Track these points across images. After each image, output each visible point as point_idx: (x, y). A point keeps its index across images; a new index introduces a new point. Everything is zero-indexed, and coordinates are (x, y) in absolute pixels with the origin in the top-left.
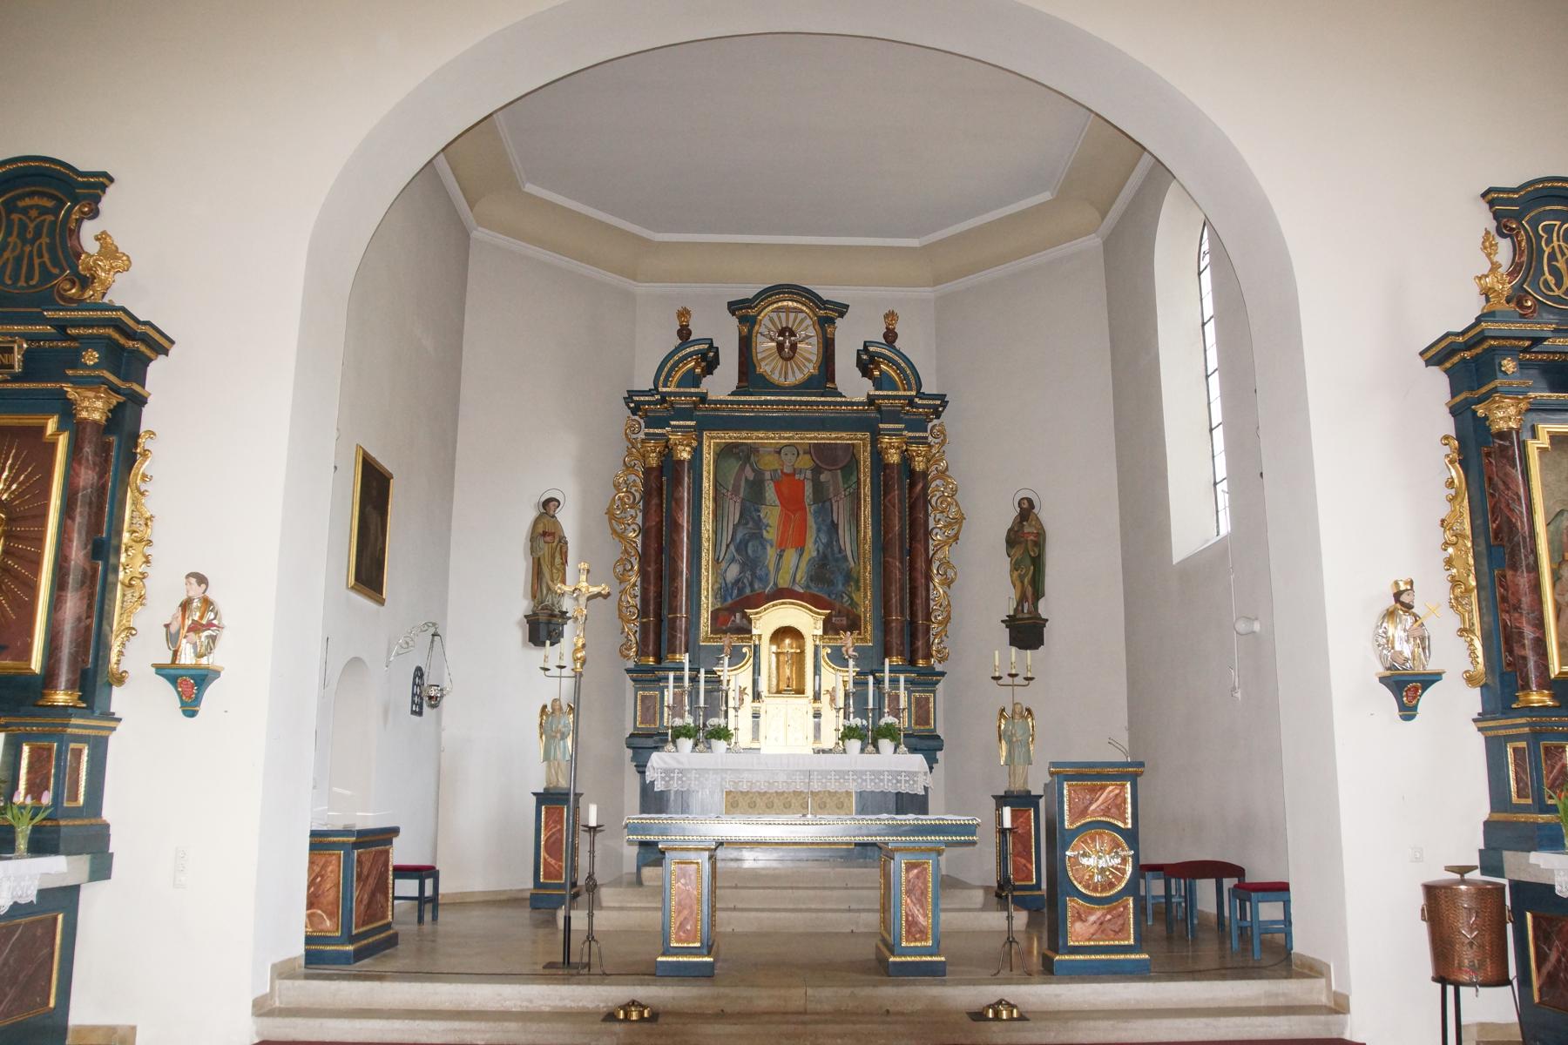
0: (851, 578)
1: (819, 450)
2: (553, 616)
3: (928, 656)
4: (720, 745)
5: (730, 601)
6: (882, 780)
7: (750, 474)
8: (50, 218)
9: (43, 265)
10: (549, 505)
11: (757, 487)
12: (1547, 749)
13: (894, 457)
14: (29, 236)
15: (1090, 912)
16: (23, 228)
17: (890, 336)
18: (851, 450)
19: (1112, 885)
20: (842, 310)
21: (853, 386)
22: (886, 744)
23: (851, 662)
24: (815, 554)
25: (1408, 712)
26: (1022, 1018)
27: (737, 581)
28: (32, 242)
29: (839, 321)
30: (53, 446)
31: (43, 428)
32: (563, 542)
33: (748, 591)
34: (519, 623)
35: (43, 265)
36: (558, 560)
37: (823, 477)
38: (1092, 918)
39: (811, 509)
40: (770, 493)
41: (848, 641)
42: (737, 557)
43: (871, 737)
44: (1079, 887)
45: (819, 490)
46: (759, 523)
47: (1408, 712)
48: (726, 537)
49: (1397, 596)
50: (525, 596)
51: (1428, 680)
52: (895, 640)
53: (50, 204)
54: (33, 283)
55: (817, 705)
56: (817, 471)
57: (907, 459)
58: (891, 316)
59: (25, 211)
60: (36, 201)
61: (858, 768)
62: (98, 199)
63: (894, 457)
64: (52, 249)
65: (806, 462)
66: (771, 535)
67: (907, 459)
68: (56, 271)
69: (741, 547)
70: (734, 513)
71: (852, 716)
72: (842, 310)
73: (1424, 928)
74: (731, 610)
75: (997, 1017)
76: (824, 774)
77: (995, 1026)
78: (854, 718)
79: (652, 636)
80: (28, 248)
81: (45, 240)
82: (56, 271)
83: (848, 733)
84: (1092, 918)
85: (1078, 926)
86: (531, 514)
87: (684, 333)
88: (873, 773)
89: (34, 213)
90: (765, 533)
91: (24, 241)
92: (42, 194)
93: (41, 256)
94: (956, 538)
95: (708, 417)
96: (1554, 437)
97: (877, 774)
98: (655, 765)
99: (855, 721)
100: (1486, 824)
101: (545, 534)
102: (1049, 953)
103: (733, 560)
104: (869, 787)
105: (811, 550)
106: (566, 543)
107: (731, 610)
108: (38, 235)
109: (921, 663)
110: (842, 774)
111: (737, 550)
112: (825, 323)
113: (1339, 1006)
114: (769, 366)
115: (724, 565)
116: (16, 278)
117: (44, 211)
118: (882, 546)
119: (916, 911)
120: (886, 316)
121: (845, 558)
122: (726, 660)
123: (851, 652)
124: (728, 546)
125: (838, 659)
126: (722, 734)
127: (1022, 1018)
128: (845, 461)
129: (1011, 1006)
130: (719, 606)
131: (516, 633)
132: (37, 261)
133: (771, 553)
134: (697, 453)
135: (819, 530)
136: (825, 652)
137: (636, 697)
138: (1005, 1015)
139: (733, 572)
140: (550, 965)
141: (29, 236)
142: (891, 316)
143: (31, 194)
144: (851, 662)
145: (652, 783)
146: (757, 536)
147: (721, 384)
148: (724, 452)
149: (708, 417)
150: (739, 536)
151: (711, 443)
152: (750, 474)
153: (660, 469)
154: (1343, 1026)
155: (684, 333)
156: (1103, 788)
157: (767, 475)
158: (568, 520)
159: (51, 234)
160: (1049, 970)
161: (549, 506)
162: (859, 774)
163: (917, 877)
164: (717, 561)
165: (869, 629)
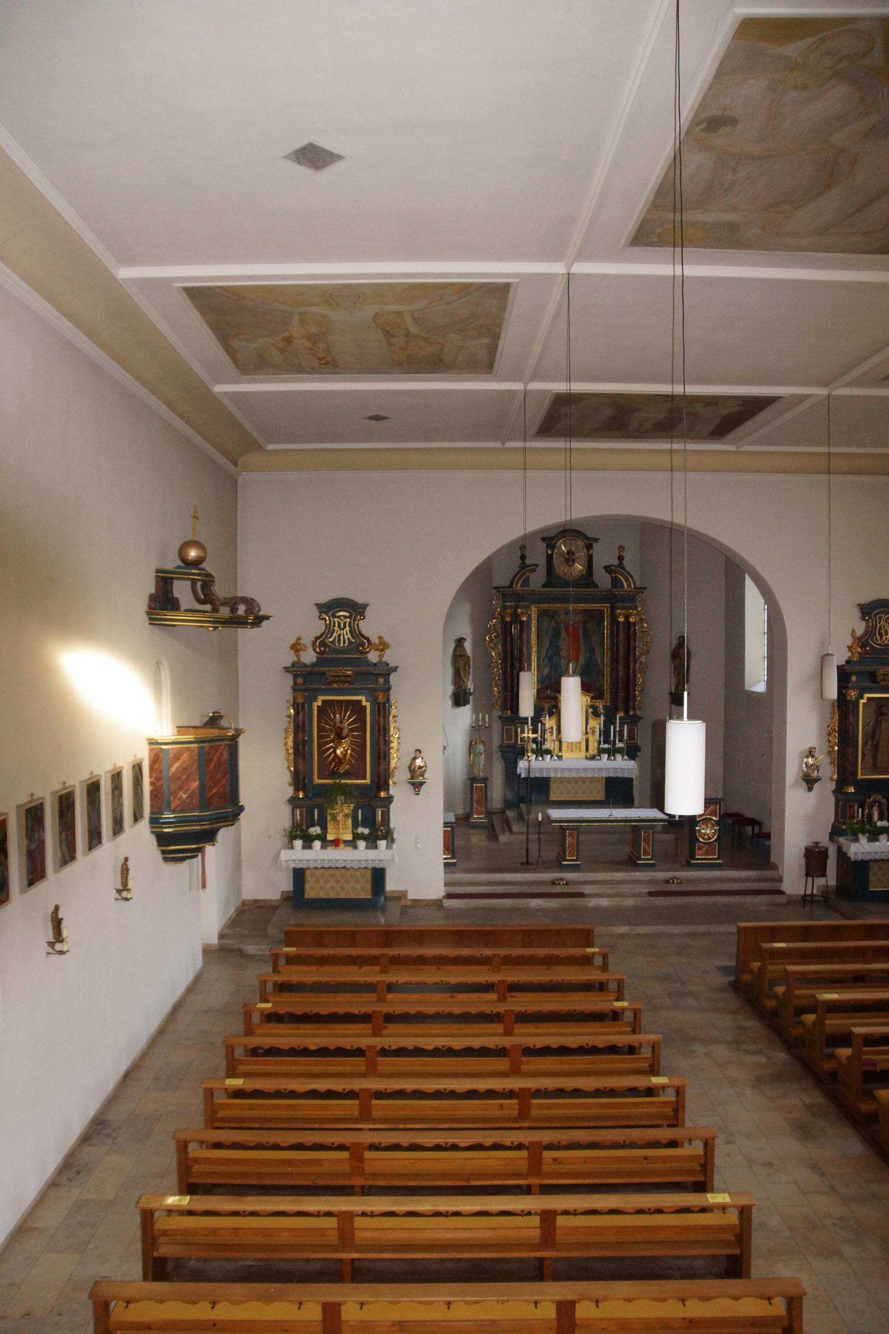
0: (601, 674)
1: (585, 612)
2: (466, 694)
3: (634, 709)
4: (549, 756)
5: (545, 684)
6: (617, 772)
7: (554, 625)
8: (348, 620)
9: (348, 638)
10: (460, 642)
11: (556, 634)
12: (850, 806)
13: (621, 619)
14: (342, 627)
15: (703, 847)
16: (339, 624)
17: (621, 558)
18: (601, 612)
19: (711, 839)
20: (596, 540)
21: (603, 580)
22: (619, 757)
23: (602, 716)
24: (584, 662)
25: (810, 789)
26: (680, 883)
27: (548, 675)
28: (343, 629)
29: (595, 545)
30: (365, 707)
31: (360, 701)
32: (468, 657)
33: (553, 680)
34: (451, 697)
35: (348, 638)
36: (467, 668)
37: (588, 626)
38: (704, 849)
39: (582, 641)
40: (563, 634)
41: (600, 704)
42: (548, 664)
43: (612, 752)
44: (701, 840)
45: (586, 631)
46: (558, 649)
47: (810, 789)
48: (543, 655)
49: (810, 752)
50: (452, 685)
51: (817, 780)
52: (620, 704)
53: (347, 614)
54: (346, 645)
55: (587, 736)
56: (585, 622)
57: (627, 617)
58: (621, 548)
59: (339, 617)
60: (342, 613)
61: (608, 767)
62: (364, 613)
63: (621, 619)
64: (351, 631)
65: (580, 618)
66: (563, 653)
67: (627, 617)
68: (353, 640)
69: (550, 659)
70: (546, 644)
71: (602, 743)
72: (596, 540)
73: (804, 859)
74: (546, 688)
75: (673, 882)
76: (593, 770)
77: (673, 886)
78: (604, 744)
79: (509, 701)
80: (342, 632)
81: (347, 629)
82: (353, 640)
83: (601, 751)
84: (704, 849)
85: (700, 852)
86: (453, 645)
87: (523, 557)
88: (613, 769)
89: (342, 618)
90: (561, 653)
91: (341, 629)
92: (344, 611)
93: (347, 635)
94: (648, 651)
95: (536, 598)
96: (868, 699)
97: (615, 769)
98: (521, 767)
99: (606, 746)
100: (832, 824)
101: (461, 656)
102: (690, 860)
103: (546, 666)
104: (612, 775)
105: (582, 660)
106: (469, 659)
107: (546, 688)
108: (345, 627)
109: (631, 713)
110: (600, 770)
111: (549, 661)
112: (589, 547)
113: (780, 880)
114: (561, 569)
115: (542, 668)
116: (339, 642)
117: (345, 617)
118: (615, 660)
119: (646, 846)
120: (619, 548)
121: (598, 664)
122: (547, 716)
123: (602, 711)
124: (544, 659)
125: (596, 714)
126: (548, 752)
127: (680, 883)
128: (598, 617)
129: (678, 879)
130: (540, 687)
131: (449, 702)
132: (346, 637)
133: (563, 661)
134: (529, 617)
135: (585, 651)
136: (590, 710)
137: (503, 730)
138: (676, 882)
139: (546, 671)
140: (522, 864)
141: (342, 627)
142: (621, 548)
143: (340, 611)
144: (602, 716)
145: (520, 774)
146: (557, 654)
147: (537, 579)
148: (542, 614)
149: (536, 598)
150: (549, 654)
151: (534, 611)
152: (554, 625)
153: (511, 622)
154: (781, 886)
155: (523, 557)
156: (710, 807)
157: (562, 625)
158: (468, 646)
159: (350, 626)
160: (689, 865)
161: (460, 642)
162: (607, 769)
163: (647, 836)
164: (538, 665)
165: (607, 696)
